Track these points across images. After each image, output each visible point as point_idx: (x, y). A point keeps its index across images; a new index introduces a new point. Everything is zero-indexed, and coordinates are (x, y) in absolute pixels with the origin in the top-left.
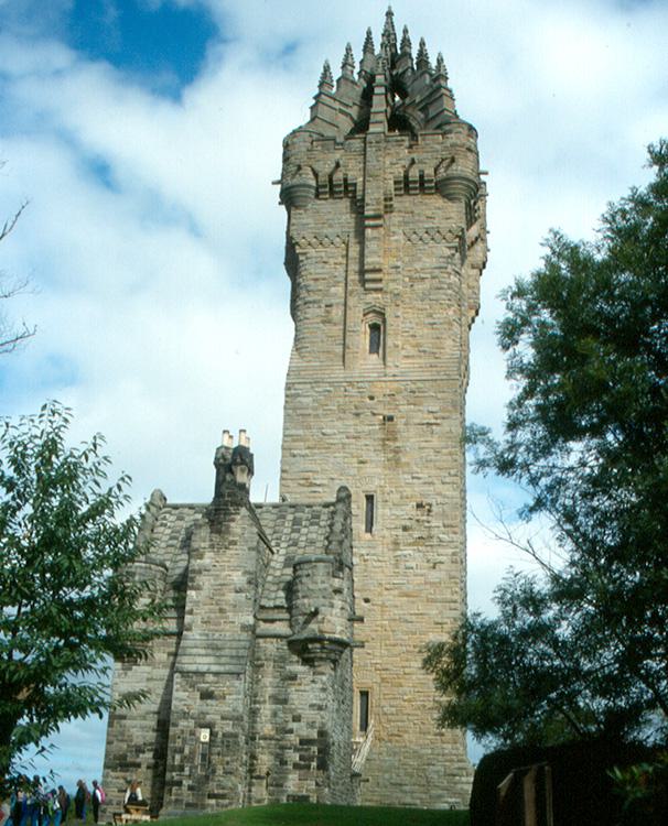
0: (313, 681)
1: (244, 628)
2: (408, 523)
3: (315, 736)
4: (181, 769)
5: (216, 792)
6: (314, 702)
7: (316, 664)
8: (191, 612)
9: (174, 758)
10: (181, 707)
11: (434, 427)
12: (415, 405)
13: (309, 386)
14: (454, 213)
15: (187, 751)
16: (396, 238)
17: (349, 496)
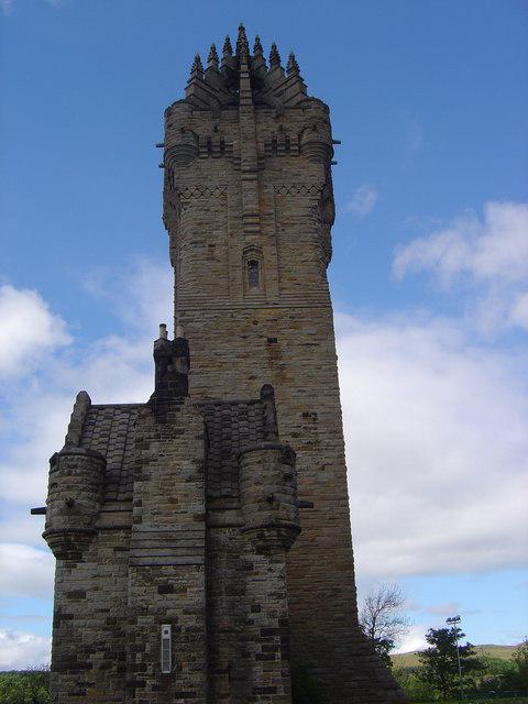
0: (270, 570)
1: (197, 518)
3: (277, 625)
4: (143, 668)
6: (273, 591)
8: (139, 504)
9: (134, 657)
11: (313, 348)
15: (148, 648)
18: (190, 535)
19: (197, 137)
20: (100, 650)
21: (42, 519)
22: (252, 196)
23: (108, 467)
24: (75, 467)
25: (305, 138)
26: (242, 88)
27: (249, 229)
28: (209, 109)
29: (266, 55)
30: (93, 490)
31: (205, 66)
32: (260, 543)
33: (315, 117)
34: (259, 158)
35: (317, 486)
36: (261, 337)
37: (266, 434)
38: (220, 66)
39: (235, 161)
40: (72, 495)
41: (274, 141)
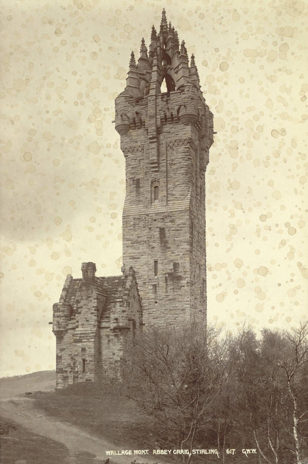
14: (186, 131)
22: (154, 152)
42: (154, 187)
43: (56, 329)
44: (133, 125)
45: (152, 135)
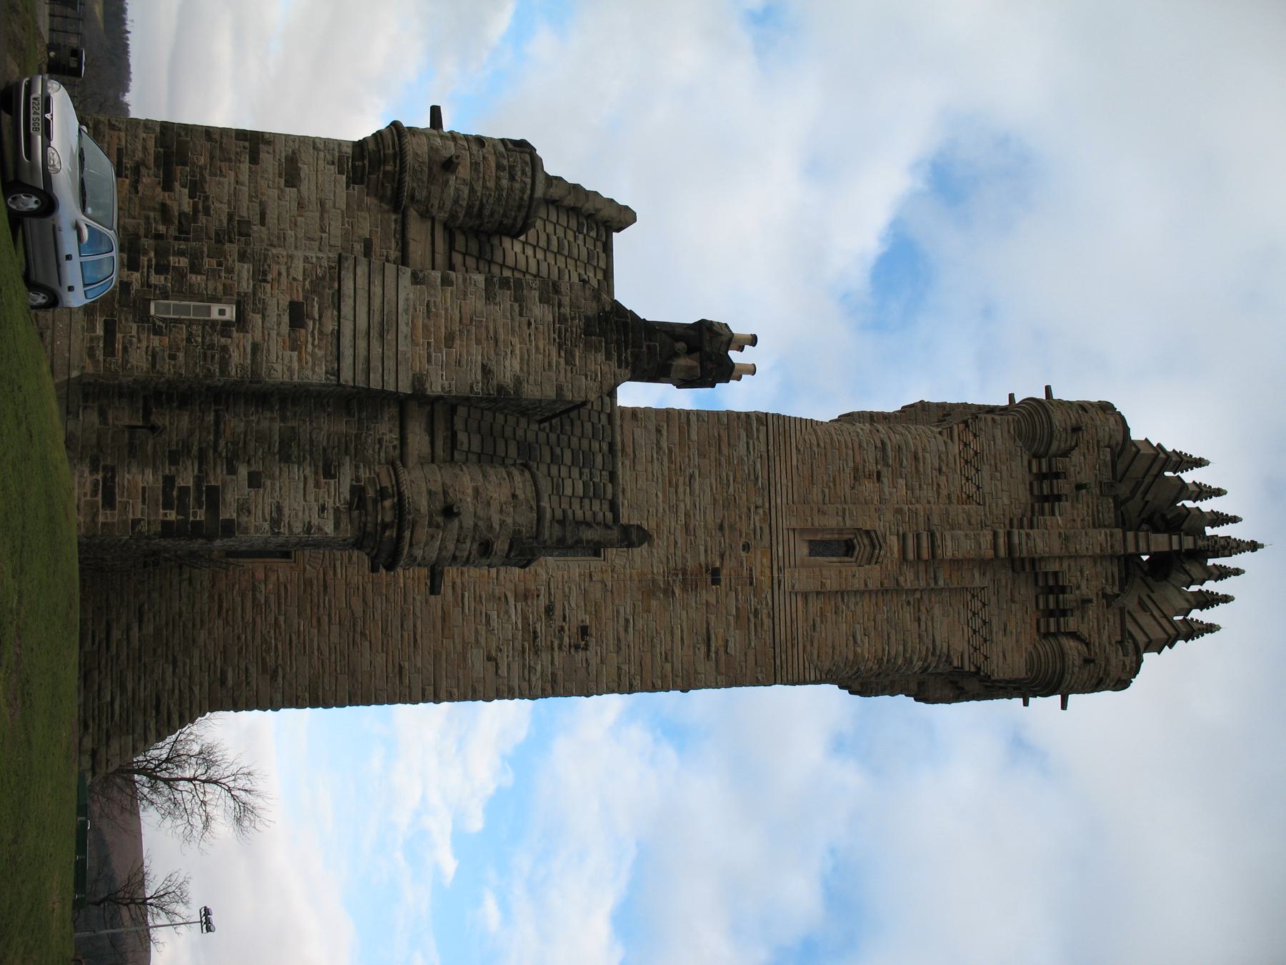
1: (419, 381)
2: (558, 612)
4: (161, 269)
5: (119, 336)
6: (286, 511)
7: (356, 513)
8: (446, 282)
9: (181, 253)
10: (275, 268)
11: (703, 649)
12: (737, 617)
13: (763, 448)
15: (196, 279)
16: (977, 575)
17: (631, 545)
18: (390, 364)
19: (1066, 454)
20: (195, 205)
21: (424, 122)
22: (967, 548)
23: (507, 242)
24: (512, 178)
25: (1070, 645)
26: (1152, 536)
27: (910, 543)
28: (1114, 477)
29: (1210, 586)
30: (470, 207)
31: (1189, 477)
32: (371, 493)
33: (1107, 660)
34: (1033, 561)
35: (459, 648)
36: (722, 556)
37: (562, 522)
38: (1189, 504)
39: (1029, 521)
40: (464, 171)
41: (1063, 590)
42: (851, 540)
43: (411, 145)
44: (1044, 469)
45: (1020, 544)
